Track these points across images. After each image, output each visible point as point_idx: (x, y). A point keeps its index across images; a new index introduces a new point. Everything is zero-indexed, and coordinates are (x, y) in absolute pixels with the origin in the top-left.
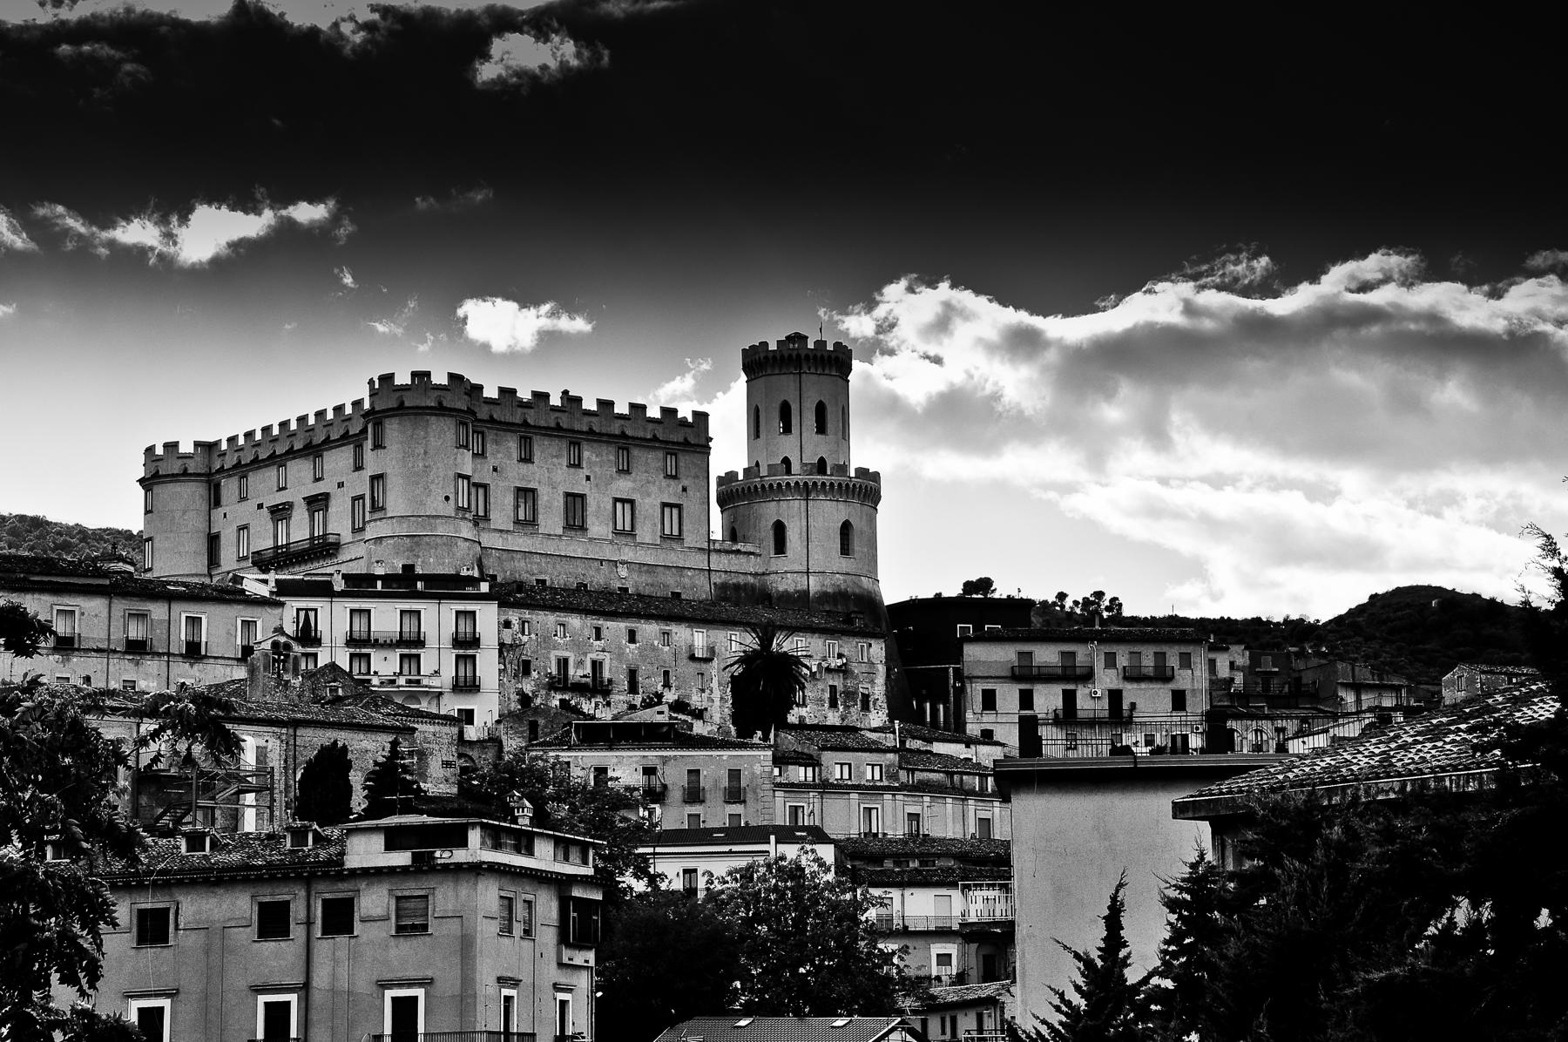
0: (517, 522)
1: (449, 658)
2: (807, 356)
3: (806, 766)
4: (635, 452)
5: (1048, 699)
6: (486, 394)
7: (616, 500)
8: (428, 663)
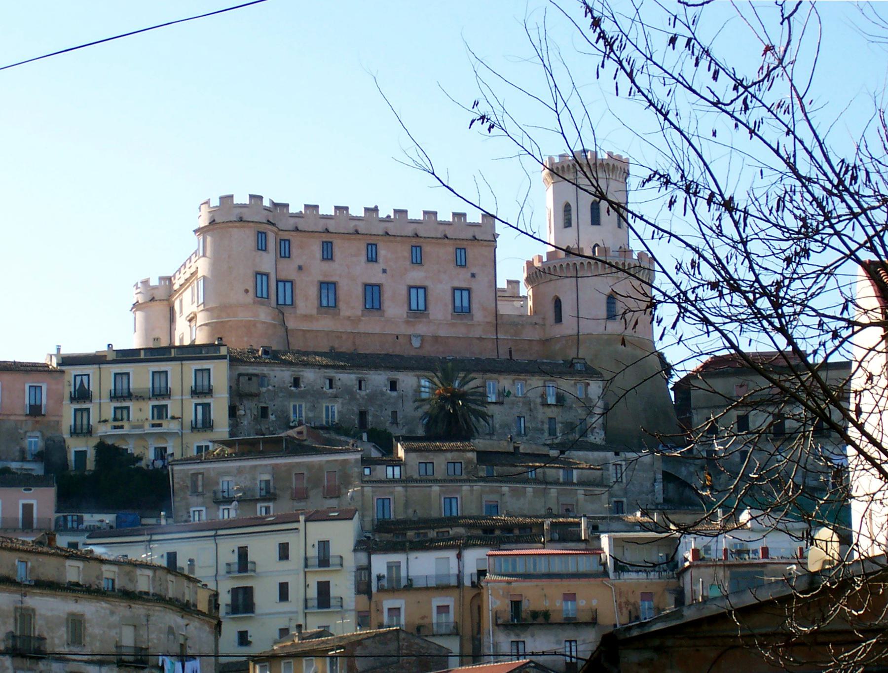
1: (191, 403)
2: (602, 165)
3: (393, 466)
6: (292, 210)
7: (410, 287)
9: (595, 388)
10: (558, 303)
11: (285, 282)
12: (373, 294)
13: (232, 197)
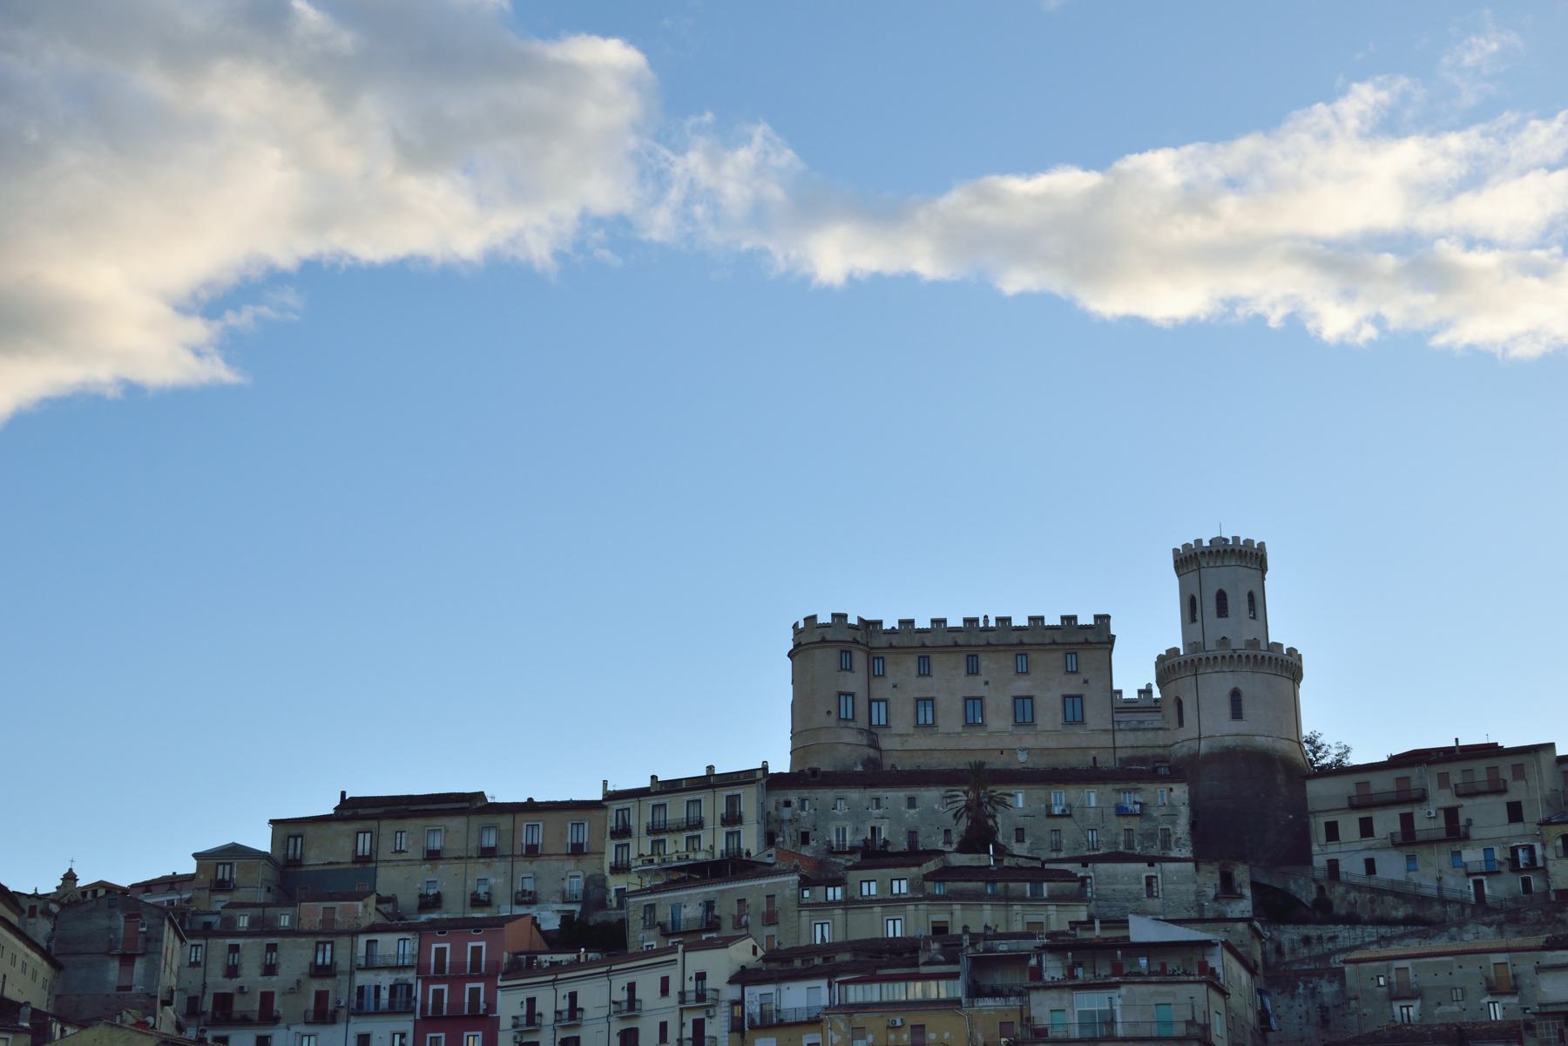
0: (917, 725)
1: (722, 833)
3: (834, 886)
4: (1034, 656)
5: (1387, 822)
7: (1015, 698)
8: (706, 839)
9: (1180, 792)
10: (1179, 703)
11: (879, 701)
12: (974, 707)
13: (814, 617)
